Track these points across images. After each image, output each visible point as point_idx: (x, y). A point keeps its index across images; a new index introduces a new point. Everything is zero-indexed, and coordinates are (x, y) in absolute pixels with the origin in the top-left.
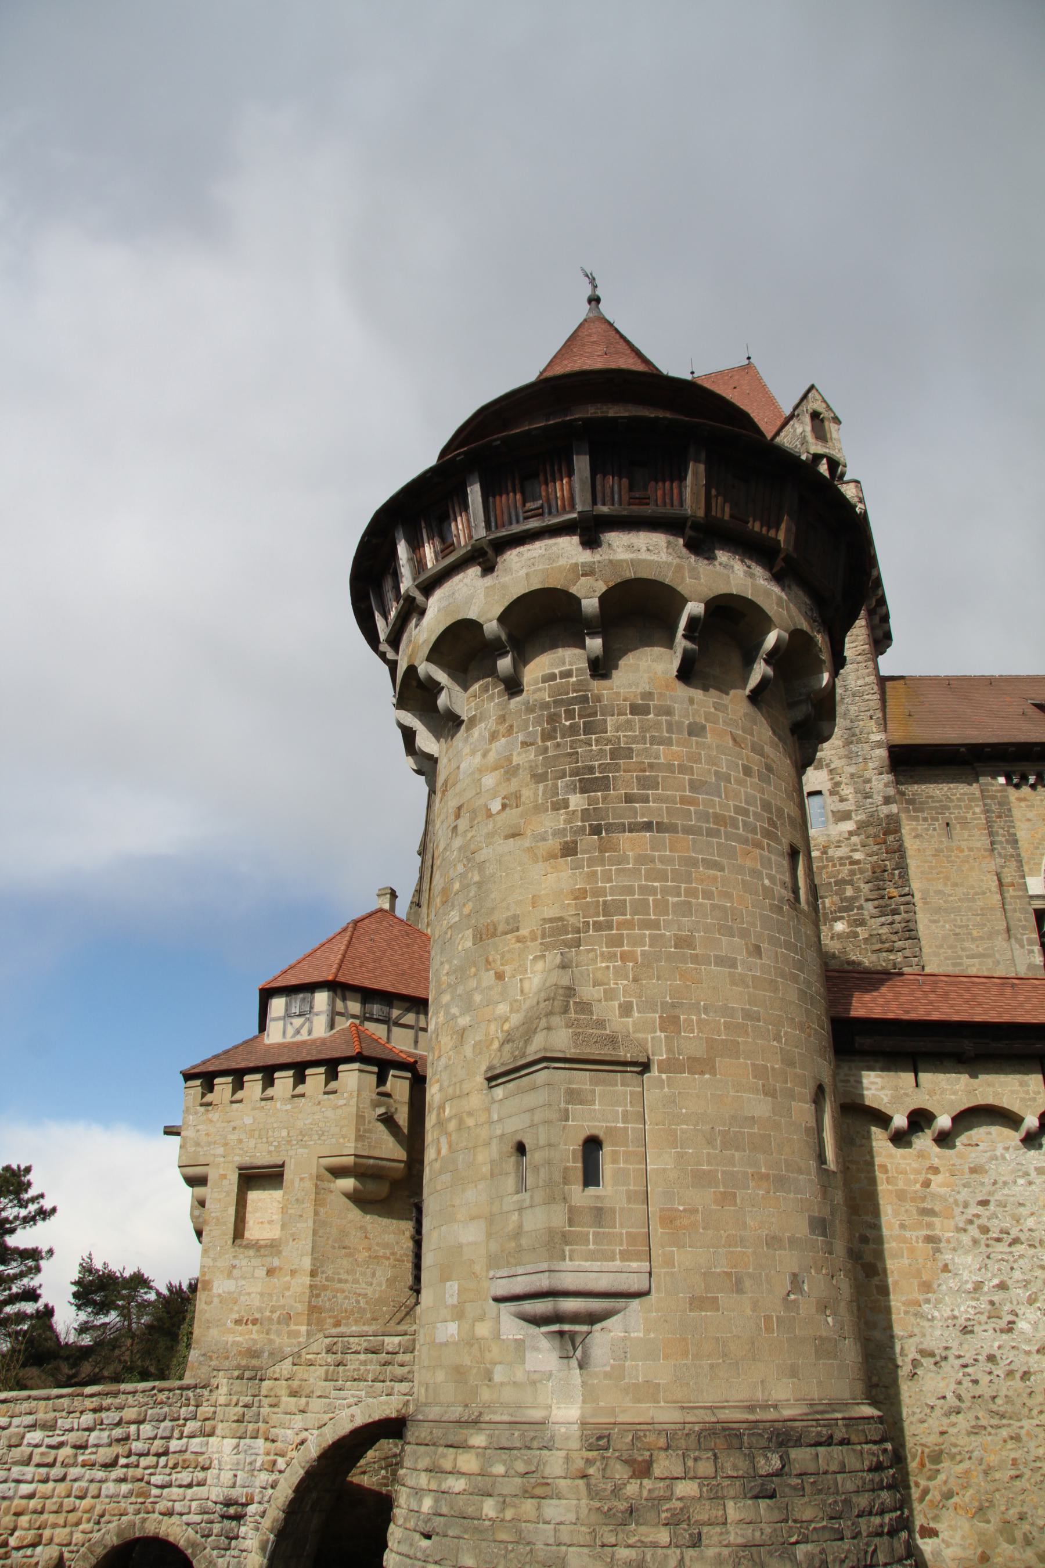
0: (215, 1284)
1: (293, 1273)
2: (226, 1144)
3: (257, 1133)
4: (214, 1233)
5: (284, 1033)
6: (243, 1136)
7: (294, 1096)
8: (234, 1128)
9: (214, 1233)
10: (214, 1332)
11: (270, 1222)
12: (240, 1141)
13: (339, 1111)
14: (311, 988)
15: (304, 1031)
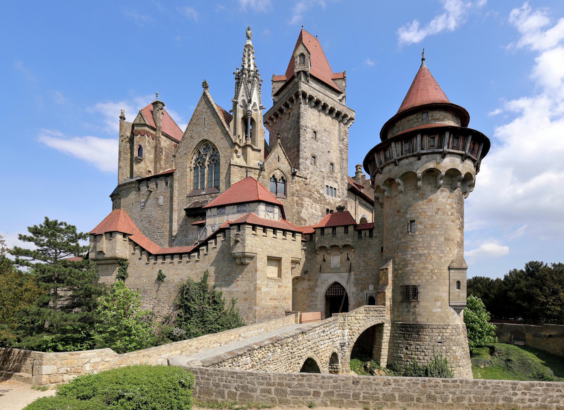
0: (262, 289)
1: (286, 287)
2: (262, 248)
3: (272, 247)
4: (261, 274)
5: (265, 216)
6: (268, 247)
7: (283, 239)
8: (265, 244)
9: (261, 274)
10: (263, 302)
11: (272, 272)
12: (267, 248)
13: (296, 246)
14: (273, 205)
15: (272, 218)
